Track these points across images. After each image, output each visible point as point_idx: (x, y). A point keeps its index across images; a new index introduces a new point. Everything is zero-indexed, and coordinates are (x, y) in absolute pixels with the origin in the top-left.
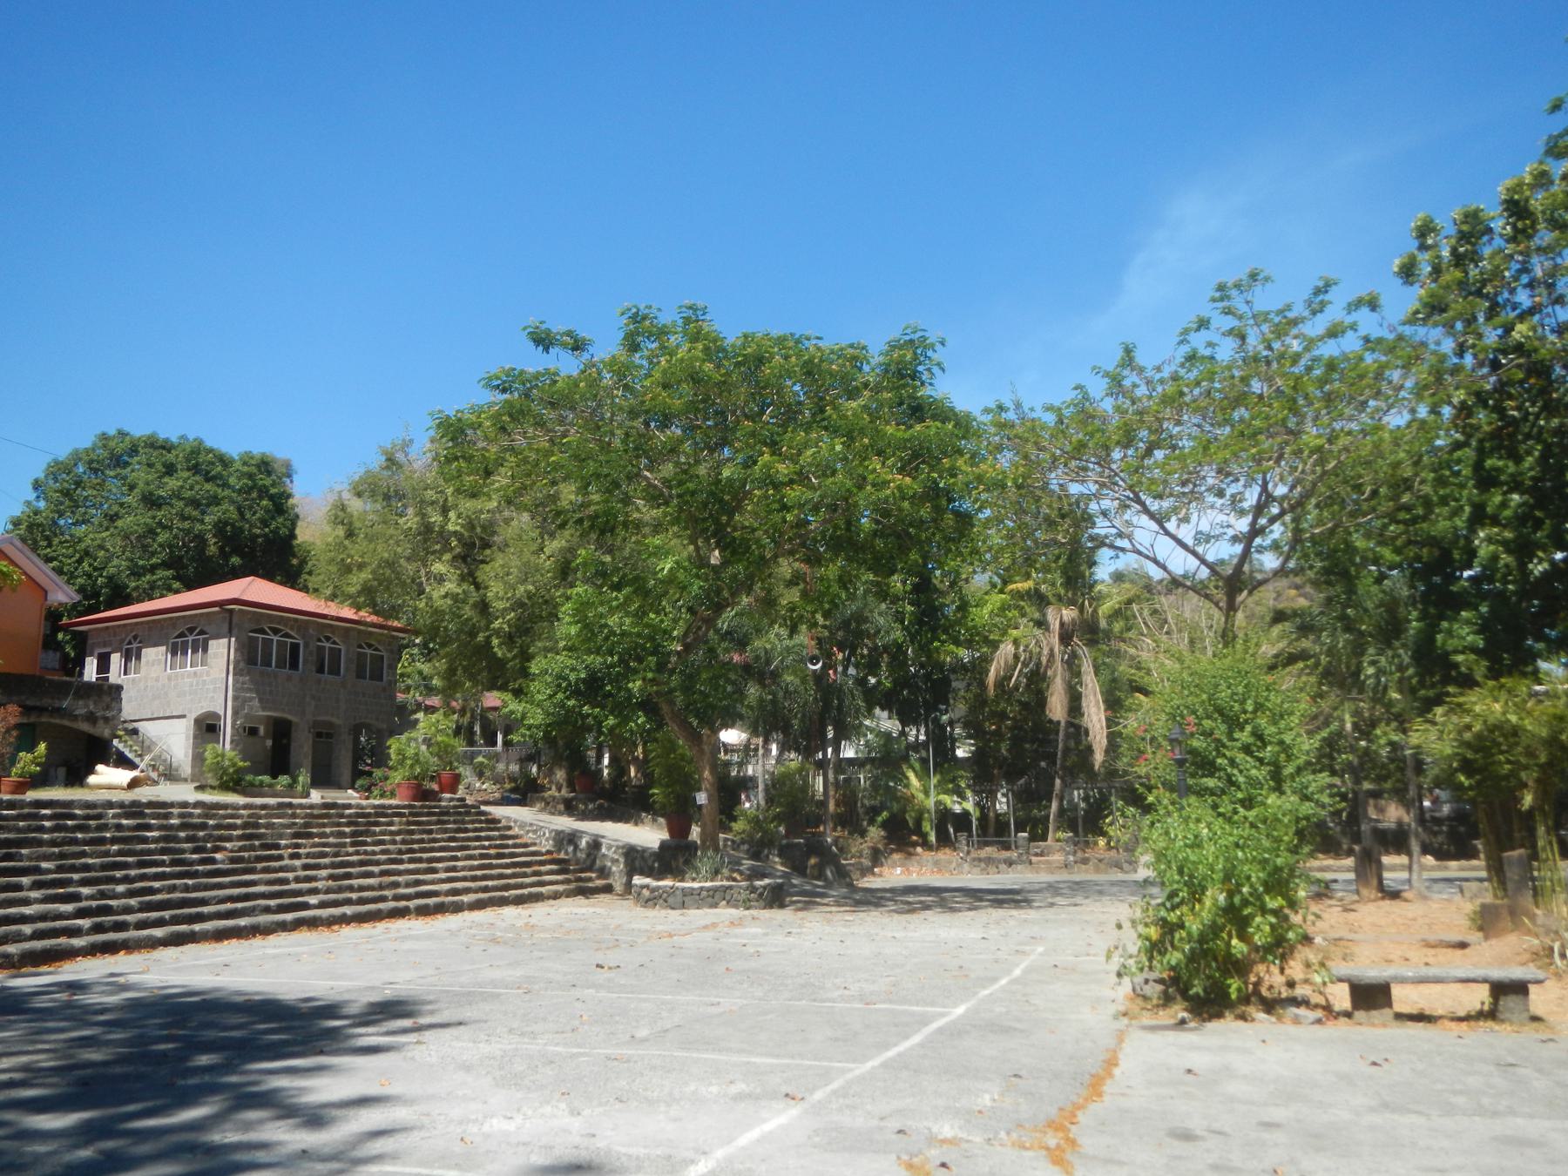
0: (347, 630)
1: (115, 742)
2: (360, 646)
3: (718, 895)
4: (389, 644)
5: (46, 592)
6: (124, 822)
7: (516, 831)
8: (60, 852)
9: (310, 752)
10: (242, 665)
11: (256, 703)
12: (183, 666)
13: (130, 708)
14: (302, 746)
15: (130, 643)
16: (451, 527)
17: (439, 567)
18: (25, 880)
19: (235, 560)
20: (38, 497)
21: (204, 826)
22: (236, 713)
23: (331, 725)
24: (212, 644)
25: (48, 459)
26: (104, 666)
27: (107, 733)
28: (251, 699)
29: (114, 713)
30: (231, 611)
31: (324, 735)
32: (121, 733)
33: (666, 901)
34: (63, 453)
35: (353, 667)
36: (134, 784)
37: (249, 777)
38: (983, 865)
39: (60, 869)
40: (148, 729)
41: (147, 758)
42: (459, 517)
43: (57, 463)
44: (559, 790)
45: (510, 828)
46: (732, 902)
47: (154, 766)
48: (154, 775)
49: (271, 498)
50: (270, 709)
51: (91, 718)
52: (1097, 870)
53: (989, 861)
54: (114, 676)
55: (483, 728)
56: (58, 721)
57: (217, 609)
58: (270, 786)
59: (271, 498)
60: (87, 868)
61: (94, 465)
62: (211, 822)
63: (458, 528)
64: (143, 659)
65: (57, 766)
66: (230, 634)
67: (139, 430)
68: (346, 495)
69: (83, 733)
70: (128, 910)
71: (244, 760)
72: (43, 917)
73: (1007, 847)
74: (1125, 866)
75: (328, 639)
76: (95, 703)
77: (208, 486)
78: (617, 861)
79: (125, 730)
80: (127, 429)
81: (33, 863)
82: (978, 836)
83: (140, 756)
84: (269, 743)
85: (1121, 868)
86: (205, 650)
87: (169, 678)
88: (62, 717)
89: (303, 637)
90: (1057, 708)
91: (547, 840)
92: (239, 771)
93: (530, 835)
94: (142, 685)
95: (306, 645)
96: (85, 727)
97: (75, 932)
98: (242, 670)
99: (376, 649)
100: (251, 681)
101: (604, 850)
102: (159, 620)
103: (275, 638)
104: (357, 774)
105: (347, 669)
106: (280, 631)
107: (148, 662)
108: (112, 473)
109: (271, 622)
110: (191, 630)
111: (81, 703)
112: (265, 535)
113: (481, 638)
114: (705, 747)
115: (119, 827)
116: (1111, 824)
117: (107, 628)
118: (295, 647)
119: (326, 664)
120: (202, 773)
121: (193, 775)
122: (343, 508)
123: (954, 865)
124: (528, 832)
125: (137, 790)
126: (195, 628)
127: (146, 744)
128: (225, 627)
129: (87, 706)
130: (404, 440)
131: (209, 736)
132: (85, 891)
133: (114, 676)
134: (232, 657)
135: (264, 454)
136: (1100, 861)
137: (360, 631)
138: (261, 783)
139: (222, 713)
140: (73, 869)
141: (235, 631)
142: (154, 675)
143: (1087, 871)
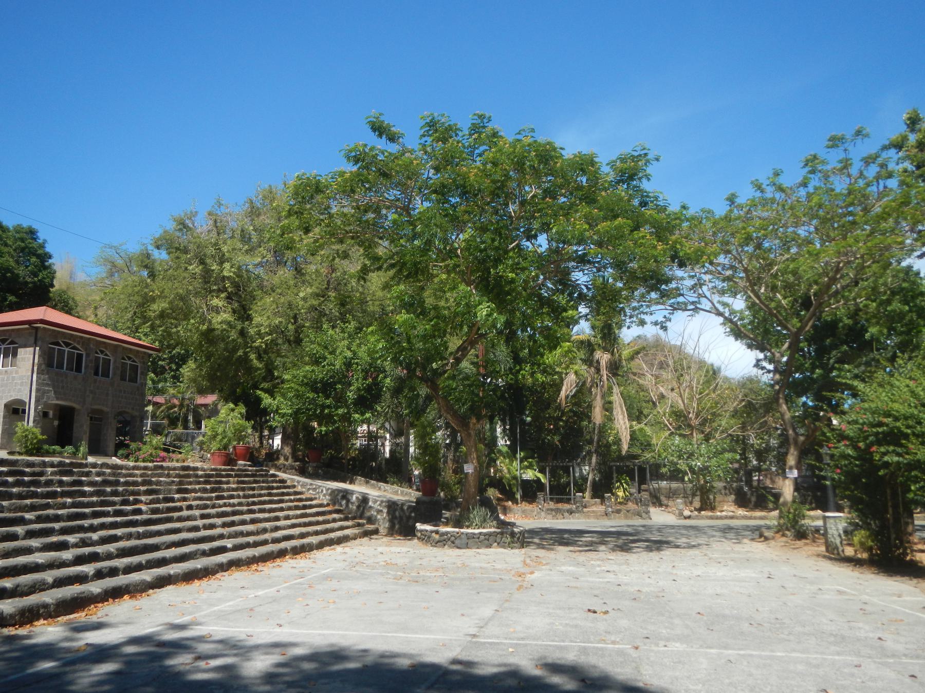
0: (116, 346)
2: (123, 359)
3: (492, 539)
4: (143, 358)
6: (65, 478)
7: (299, 489)
8: (31, 504)
10: (43, 367)
14: (82, 426)
16: (226, 273)
17: (216, 302)
18: (20, 530)
19: (12, 298)
21: (117, 483)
22: (37, 401)
23: (100, 412)
28: (49, 391)
30: (37, 328)
31: (97, 419)
33: (453, 542)
35: (119, 372)
37: (46, 447)
38: (554, 513)
39: (39, 519)
42: (232, 267)
44: (286, 460)
45: (294, 486)
46: (502, 544)
49: (39, 256)
50: (62, 399)
52: (626, 517)
53: (558, 511)
55: (194, 417)
60: (57, 518)
62: (122, 480)
63: (232, 274)
66: (35, 344)
68: (150, 247)
70: (109, 556)
71: (42, 434)
72: (51, 566)
73: (568, 501)
74: (644, 515)
75: (102, 352)
78: (381, 511)
81: (19, 514)
82: (550, 494)
84: (56, 423)
85: (641, 516)
86: (15, 355)
89: (86, 350)
90: (598, 415)
91: (324, 495)
92: (41, 442)
93: (311, 491)
95: (88, 355)
97: (81, 579)
98: (43, 370)
99: (134, 361)
100: (50, 378)
101: (370, 503)
103: (67, 349)
104: (120, 445)
105: (114, 374)
106: (70, 344)
109: (65, 338)
112: (34, 283)
113: (240, 353)
114: (472, 433)
115: (61, 483)
116: (618, 488)
118: (80, 357)
119: (101, 370)
122: (148, 256)
123: (535, 513)
124: (309, 489)
126: (6, 340)
128: (32, 340)
130: (191, 212)
132: (71, 539)
134: (36, 361)
136: (628, 511)
137: (124, 348)
138: (54, 450)
139: (27, 401)
140: (48, 519)
141: (39, 343)
143: (619, 518)
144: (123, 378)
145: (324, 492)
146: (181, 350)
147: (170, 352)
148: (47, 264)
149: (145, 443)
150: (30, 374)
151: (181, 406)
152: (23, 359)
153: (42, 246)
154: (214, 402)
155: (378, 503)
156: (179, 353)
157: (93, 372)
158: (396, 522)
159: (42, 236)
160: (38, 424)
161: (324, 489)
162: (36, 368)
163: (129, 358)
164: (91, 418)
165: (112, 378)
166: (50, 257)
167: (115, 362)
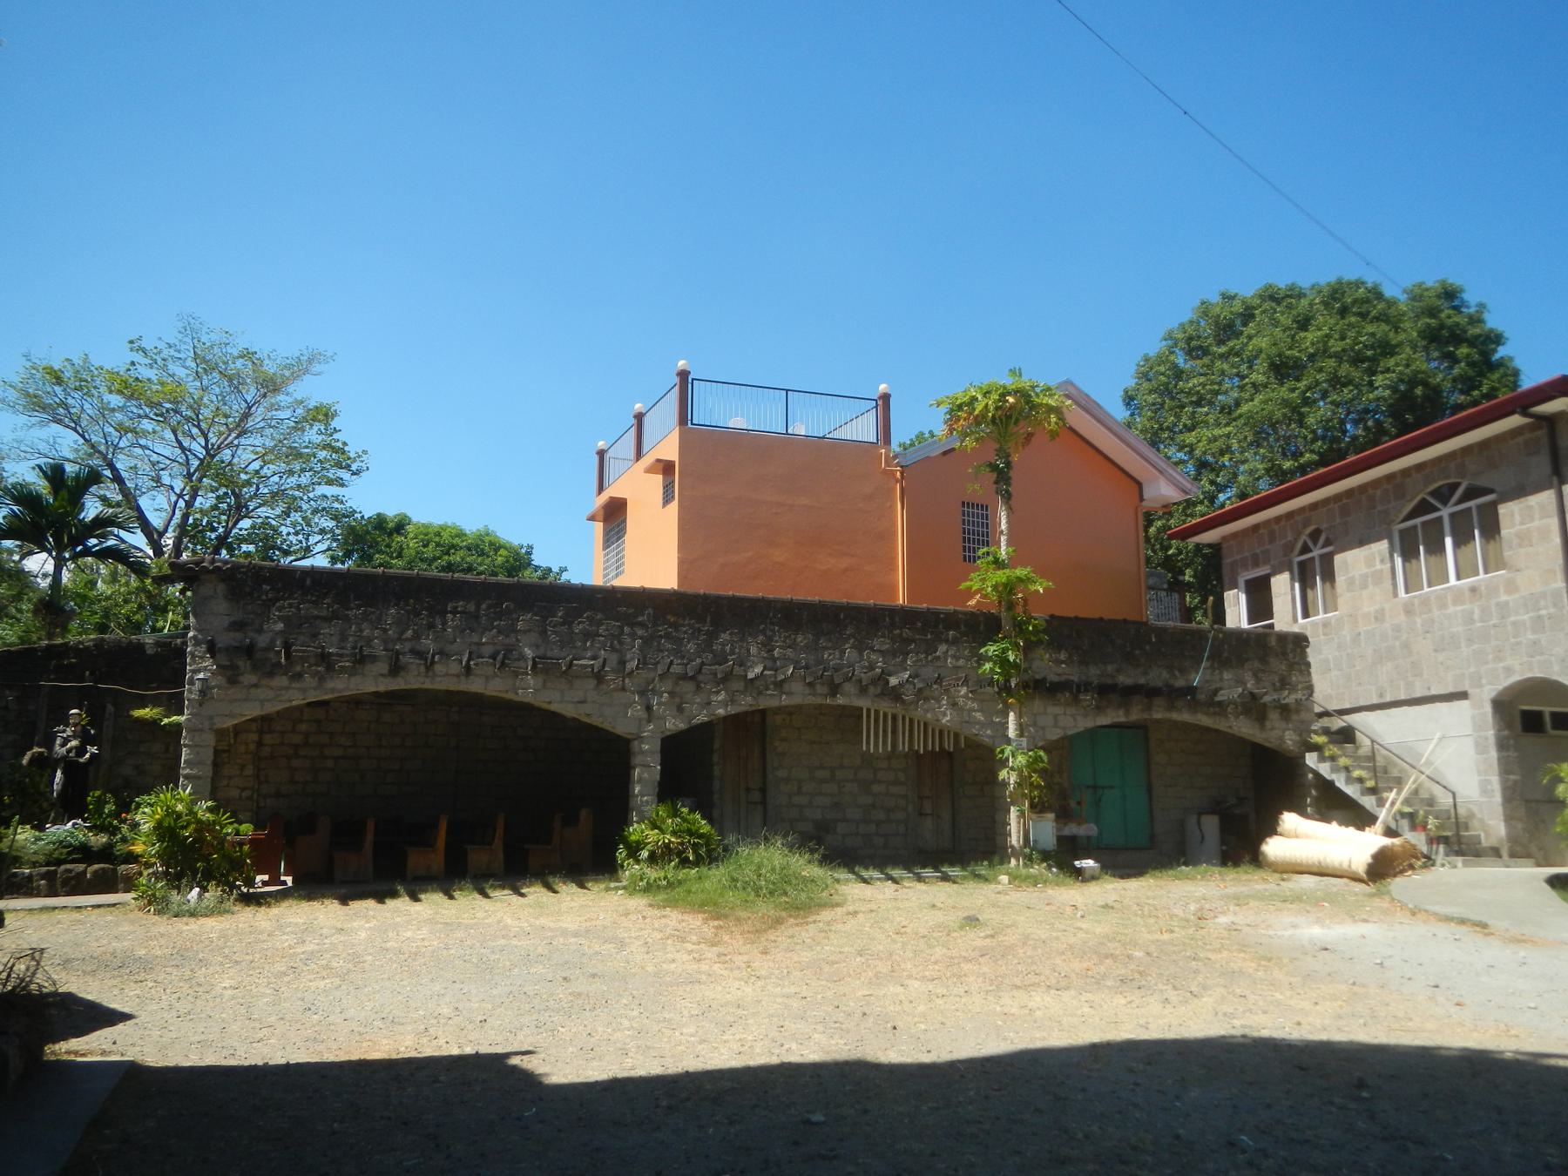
1: (1311, 759)
5: (1139, 484)
15: (1306, 549)
20: (1132, 415)
24: (1512, 514)
25: (1138, 358)
26: (1261, 605)
27: (1290, 740)
29: (1299, 695)
30: (1550, 421)
32: (1320, 739)
34: (1154, 346)
36: (1382, 868)
40: (1378, 728)
41: (1395, 799)
43: (1147, 359)
48: (1418, 840)
49: (1472, 343)
51: (1254, 708)
54: (1285, 615)
56: (1185, 716)
57: (1515, 421)
59: (1472, 343)
61: (1194, 343)
64: (1340, 579)
65: (1200, 814)
67: (1248, 289)
69: (1241, 741)
76: (1255, 675)
77: (1370, 328)
79: (1326, 731)
80: (1232, 292)
83: (1373, 791)
86: (1491, 529)
87: (1408, 610)
88: (1195, 705)
94: (1346, 633)
96: (1244, 728)
102: (1363, 488)
108: (1223, 349)
110: (1444, 495)
111: (1227, 675)
117: (1256, 528)
121: (1513, 839)
126: (1454, 487)
127: (1380, 762)
128: (1542, 463)
129: (1244, 684)
131: (1532, 740)
133: (1285, 615)
135: (1443, 282)
142: (1369, 608)
148: (1497, 356)
152: (1524, 539)
153: (1476, 320)
159: (1472, 297)
166: (1497, 339)
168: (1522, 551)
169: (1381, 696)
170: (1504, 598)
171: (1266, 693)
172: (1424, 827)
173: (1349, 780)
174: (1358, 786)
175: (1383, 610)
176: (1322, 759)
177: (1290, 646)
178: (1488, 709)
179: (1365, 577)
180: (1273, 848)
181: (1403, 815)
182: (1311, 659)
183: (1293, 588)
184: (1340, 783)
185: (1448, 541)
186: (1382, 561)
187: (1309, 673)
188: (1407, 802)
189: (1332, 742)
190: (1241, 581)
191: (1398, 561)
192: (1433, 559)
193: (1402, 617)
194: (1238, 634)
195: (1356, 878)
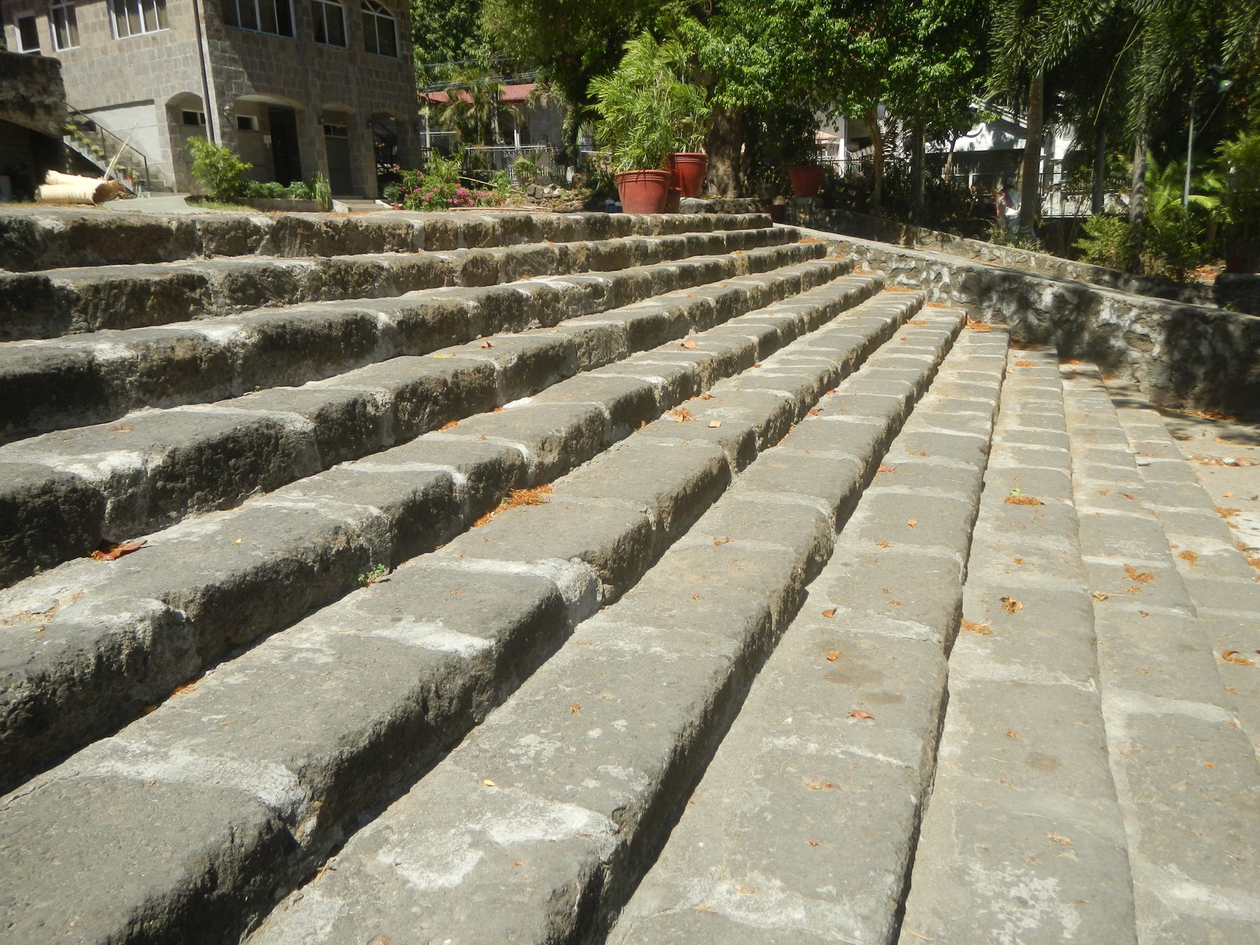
1: (67, 140)
2: (364, 6)
9: (325, 151)
10: (217, 23)
11: (245, 80)
12: (135, 29)
13: (77, 93)
22: (220, 94)
23: (342, 116)
26: (30, 38)
27: (52, 128)
31: (336, 128)
32: (72, 128)
36: (101, 195)
37: (254, 185)
40: (109, 121)
41: (113, 160)
47: (124, 171)
48: (128, 184)
51: (25, 105)
58: (283, 195)
64: (80, 24)
71: (243, 160)
76: (25, 84)
78: (1144, 338)
79: (78, 124)
83: (104, 158)
84: (268, 139)
87: (121, 49)
91: (946, 289)
93: (902, 278)
94: (85, 60)
96: (19, 118)
98: (217, 30)
99: (384, 12)
100: (233, 46)
104: (387, 178)
105: (353, 38)
107: (86, 27)
120: (191, 179)
121: (179, 182)
124: (896, 271)
125: (109, 205)
127: (109, 142)
129: (15, 88)
131: (187, 128)
134: (201, 11)
138: (271, 191)
139: (202, 95)
142: (98, 45)
144: (370, 48)
145: (946, 279)
146: (461, 10)
147: (442, 17)
149: (426, 172)
150: (195, 39)
151: (479, 103)
154: (532, 93)
155: (1134, 313)
156: (457, 17)
157: (312, 34)
158: (1200, 372)
160: (230, 140)
161: (945, 271)
162: (203, 26)
163: (376, 6)
164: (327, 130)
165: (351, 45)
167: (350, 12)
168: (177, 17)
169: (108, 101)
170: (169, 45)
171: (33, 96)
172: (131, 177)
173: (90, 152)
174: (94, 155)
175: (106, 47)
176: (73, 139)
177: (48, 67)
178: (164, 110)
179: (94, 24)
180: (45, 191)
181: (120, 171)
182: (64, 77)
183: (51, 27)
184: (85, 154)
185: (140, 6)
186: (104, 15)
187: (62, 85)
188: (119, 163)
189: (78, 129)
190: (16, 20)
191: (114, 16)
192: (133, 17)
193: (117, 52)
194: (14, 58)
195: (89, 203)
